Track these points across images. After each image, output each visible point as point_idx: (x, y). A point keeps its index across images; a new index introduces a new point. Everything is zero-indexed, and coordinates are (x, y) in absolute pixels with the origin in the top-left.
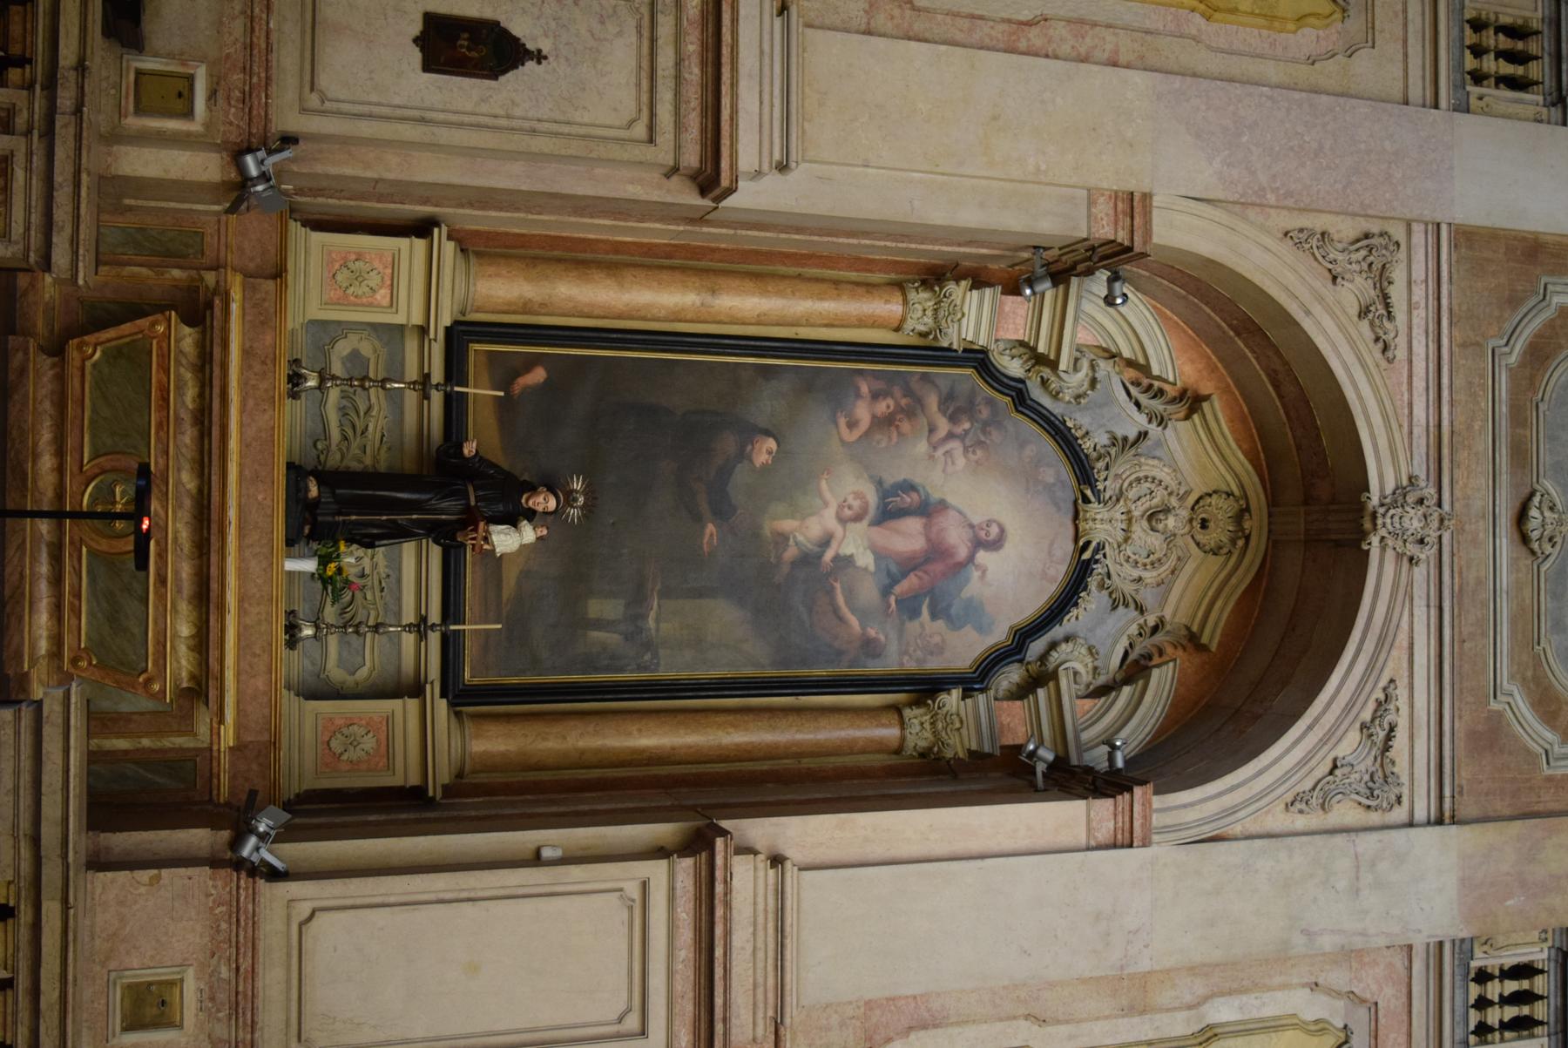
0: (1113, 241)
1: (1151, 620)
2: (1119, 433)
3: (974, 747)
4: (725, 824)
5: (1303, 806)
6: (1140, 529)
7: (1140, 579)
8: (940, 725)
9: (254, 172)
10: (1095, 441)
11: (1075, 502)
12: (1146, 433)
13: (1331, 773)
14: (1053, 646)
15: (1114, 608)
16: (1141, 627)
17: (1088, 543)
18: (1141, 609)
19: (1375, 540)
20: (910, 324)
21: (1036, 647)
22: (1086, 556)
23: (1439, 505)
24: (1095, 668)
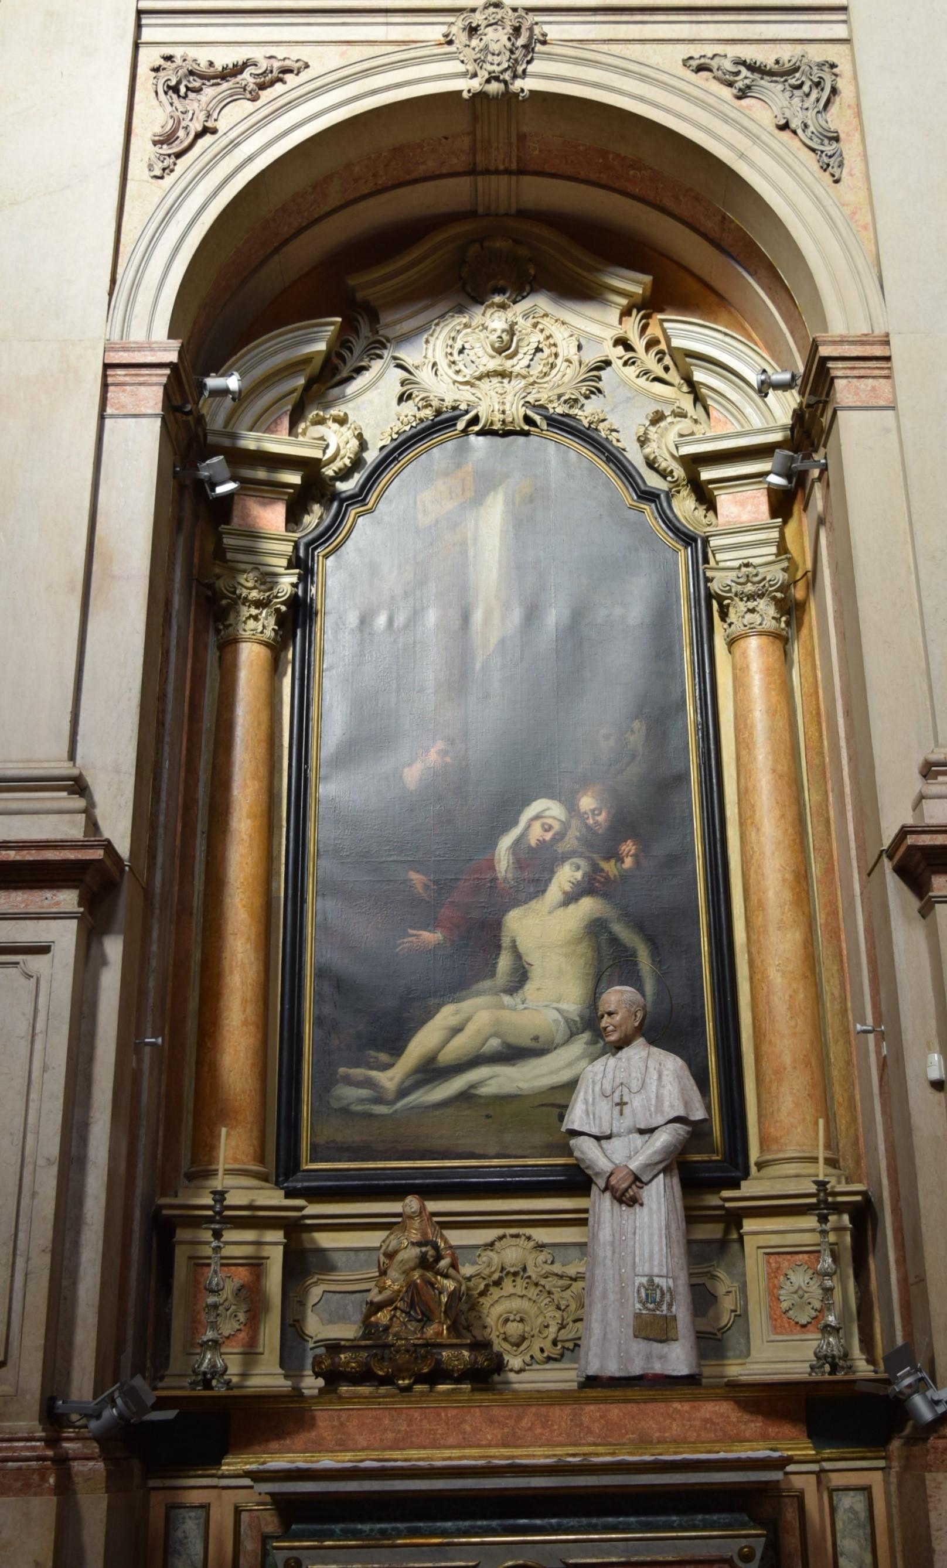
0: (166, 387)
3: (774, 550)
4: (889, 834)
8: (749, 588)
13: (795, 132)
14: (651, 464)
15: (600, 391)
16: (625, 364)
17: (528, 420)
19: (518, 84)
21: (654, 481)
24: (675, 414)
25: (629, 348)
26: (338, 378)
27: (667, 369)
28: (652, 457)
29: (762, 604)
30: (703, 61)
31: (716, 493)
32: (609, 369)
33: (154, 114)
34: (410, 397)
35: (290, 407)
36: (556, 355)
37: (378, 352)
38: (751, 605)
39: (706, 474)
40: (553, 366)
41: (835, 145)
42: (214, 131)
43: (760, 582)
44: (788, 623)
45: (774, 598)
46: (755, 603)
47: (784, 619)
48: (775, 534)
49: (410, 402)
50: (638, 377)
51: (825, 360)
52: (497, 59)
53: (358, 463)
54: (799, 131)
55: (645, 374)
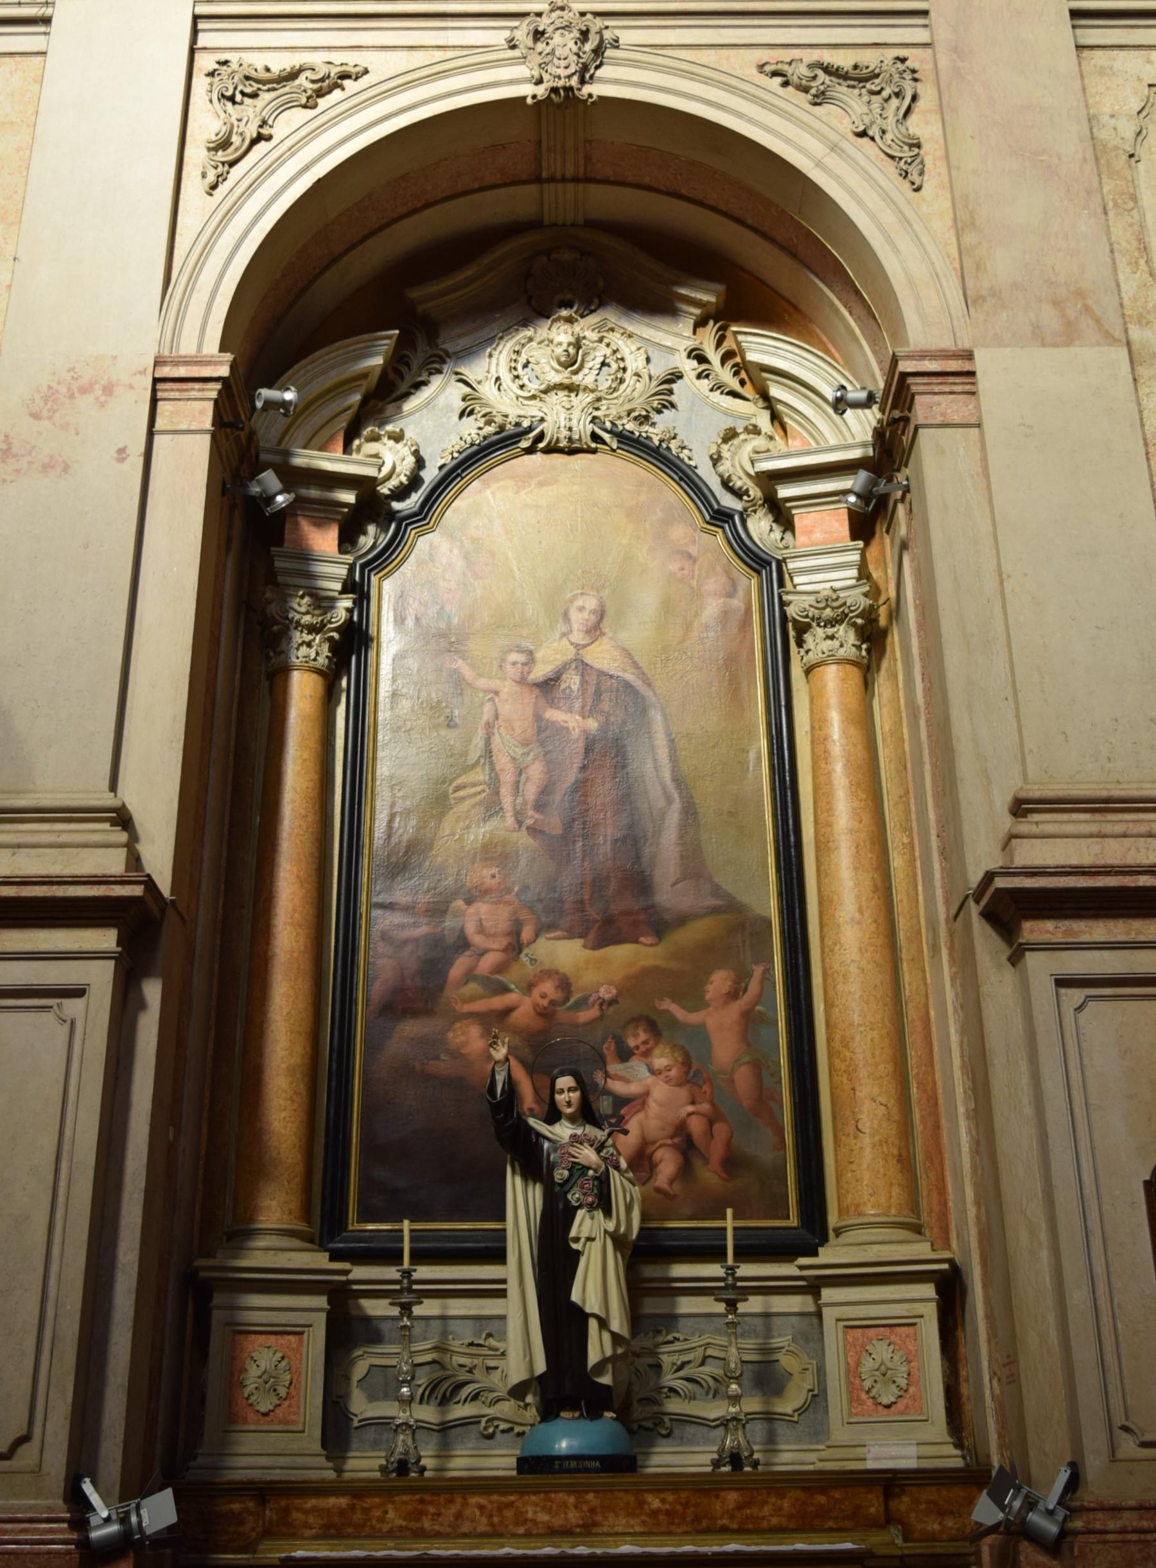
0: (216, 402)
1: (689, 367)
3: (854, 573)
4: (975, 877)
9: (114, 1528)
13: (873, 139)
14: (726, 484)
15: (673, 406)
16: (699, 377)
17: (595, 437)
18: (676, 376)
21: (728, 501)
23: (539, 15)
25: (702, 359)
26: (399, 393)
27: (742, 383)
28: (726, 475)
29: (841, 630)
30: (780, 66)
31: (794, 512)
32: (679, 382)
33: (208, 122)
34: (471, 413)
35: (344, 424)
36: (624, 370)
37: (437, 366)
38: (830, 631)
39: (784, 492)
40: (622, 381)
41: (916, 150)
42: (269, 138)
43: (838, 607)
44: (868, 651)
46: (835, 629)
47: (864, 646)
48: (855, 557)
49: (473, 417)
50: (711, 390)
51: (904, 375)
52: (563, 63)
53: (415, 481)
54: (877, 138)
55: (719, 388)
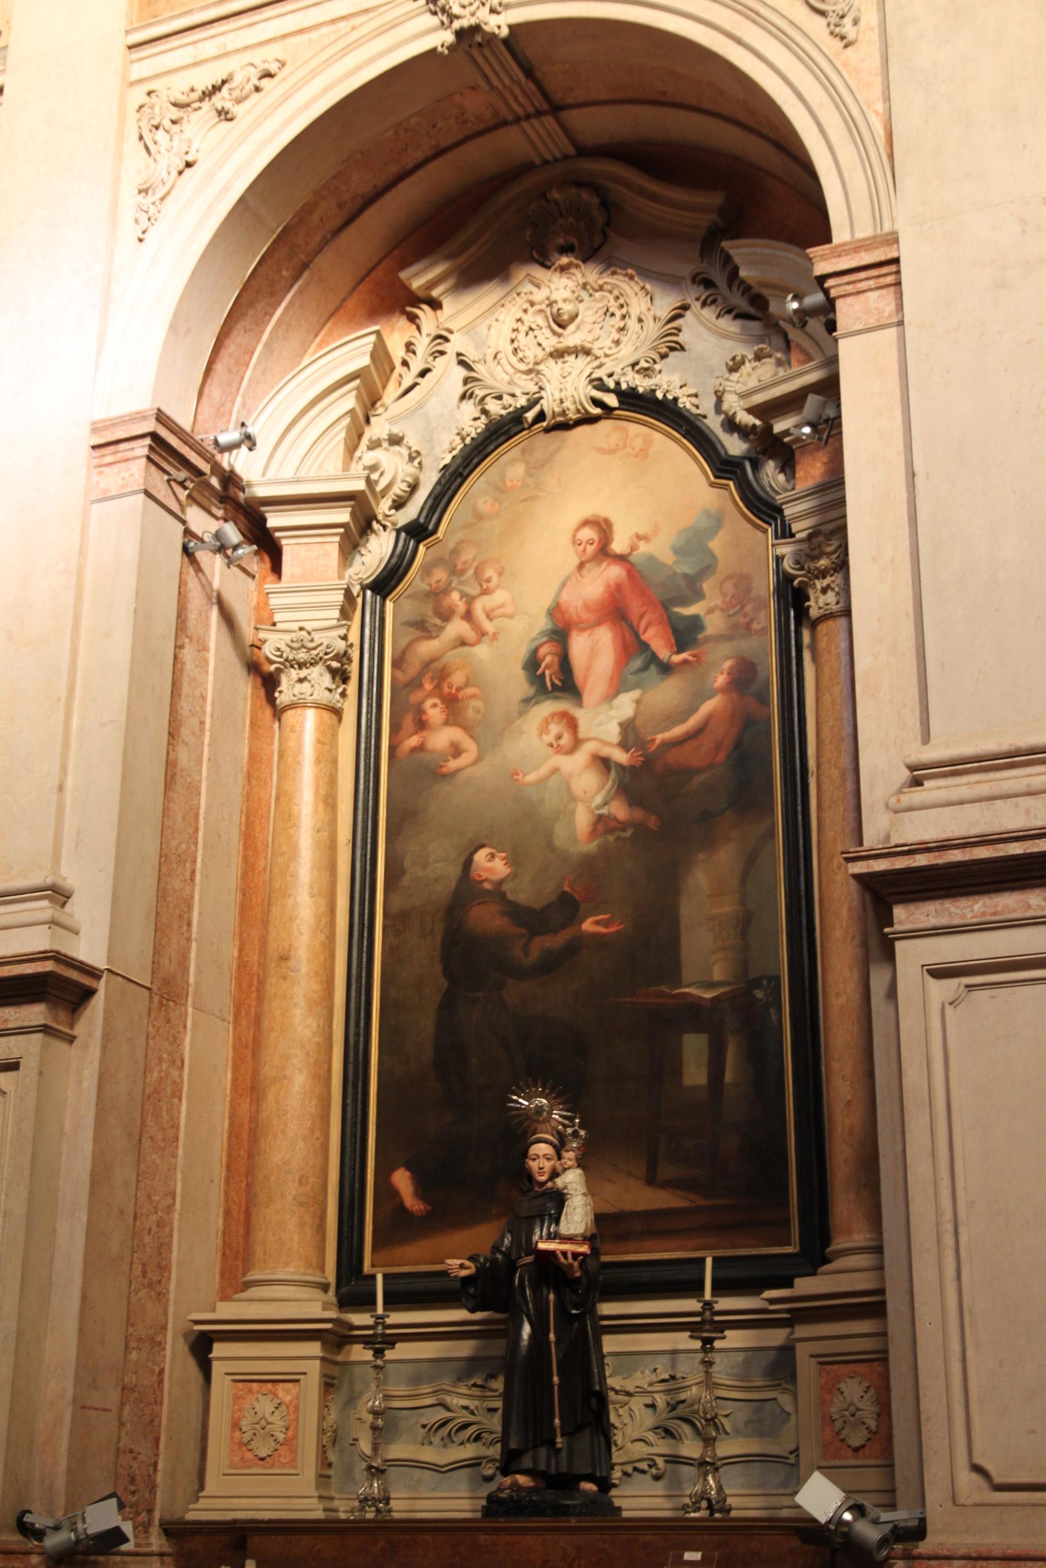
2: (460, 389)
5: (848, 21)
6: (572, 337)
7: (640, 320)
10: (469, 422)
11: (547, 430)
12: (459, 355)
20: (321, 695)
22: (612, 400)
34: (471, 396)
35: (343, 435)
45: (330, 669)
49: (472, 401)
